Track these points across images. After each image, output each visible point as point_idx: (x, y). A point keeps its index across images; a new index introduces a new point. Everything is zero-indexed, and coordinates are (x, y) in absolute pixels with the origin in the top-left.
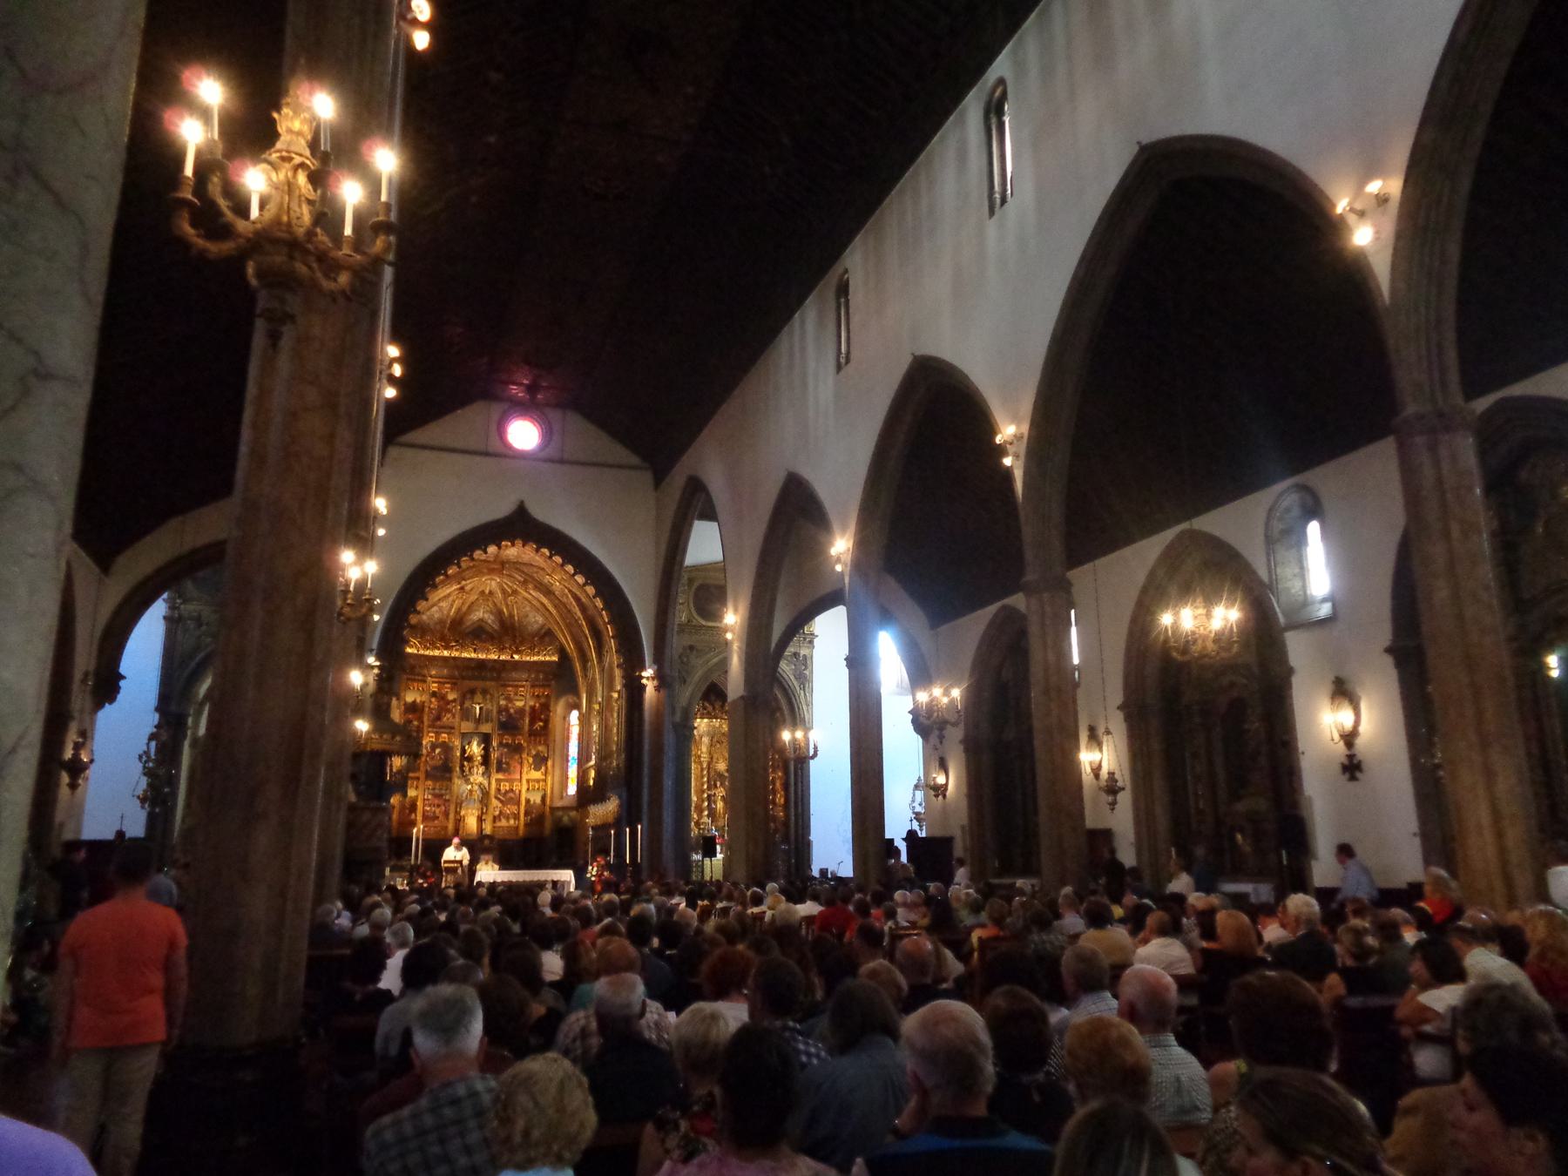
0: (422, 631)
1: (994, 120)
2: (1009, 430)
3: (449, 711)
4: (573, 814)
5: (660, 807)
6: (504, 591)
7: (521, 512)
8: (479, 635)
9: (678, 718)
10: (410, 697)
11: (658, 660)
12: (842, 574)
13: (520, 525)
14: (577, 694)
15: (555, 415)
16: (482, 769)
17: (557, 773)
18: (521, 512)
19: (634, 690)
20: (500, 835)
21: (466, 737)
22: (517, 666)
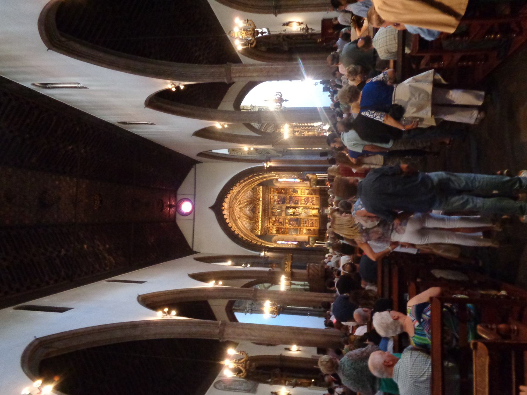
0: (253, 230)
2: (169, 85)
3: (279, 220)
4: (312, 180)
5: (311, 161)
6: (239, 204)
7: (213, 208)
8: (254, 210)
9: (280, 155)
10: (274, 232)
12: (228, 125)
13: (217, 208)
15: (179, 197)
16: (297, 209)
18: (213, 208)
19: (271, 169)
20: (318, 203)
22: (264, 199)
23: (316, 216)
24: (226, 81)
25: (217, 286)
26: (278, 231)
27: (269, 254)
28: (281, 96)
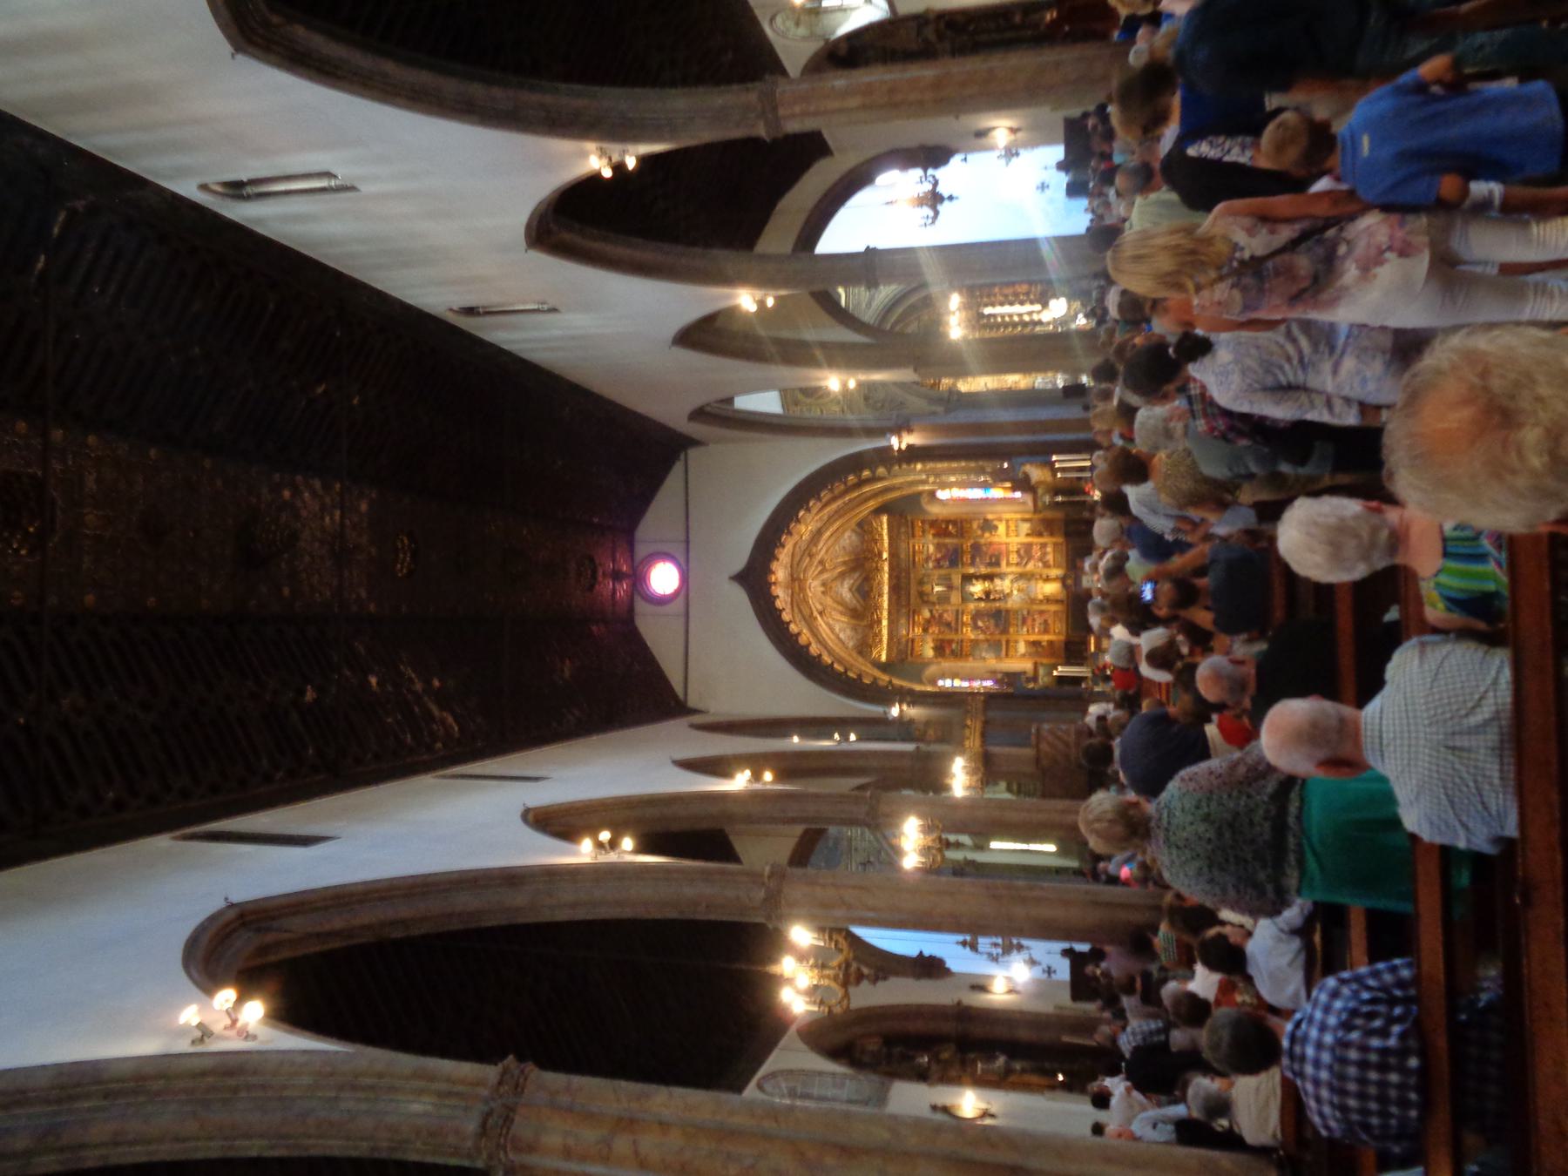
0: (864, 647)
1: (249, 190)
2: (595, 161)
3: (941, 616)
4: (1040, 491)
6: (821, 572)
9: (940, 409)
10: (929, 652)
11: (883, 432)
12: (776, 298)
13: (754, 579)
14: (920, 494)
15: (641, 551)
16: (997, 581)
17: (999, 508)
19: (912, 454)
20: (1062, 560)
21: (967, 597)
23: (1057, 601)
24: (761, 131)
25: (758, 786)
26: (940, 649)
27: (913, 712)
28: (936, 184)
